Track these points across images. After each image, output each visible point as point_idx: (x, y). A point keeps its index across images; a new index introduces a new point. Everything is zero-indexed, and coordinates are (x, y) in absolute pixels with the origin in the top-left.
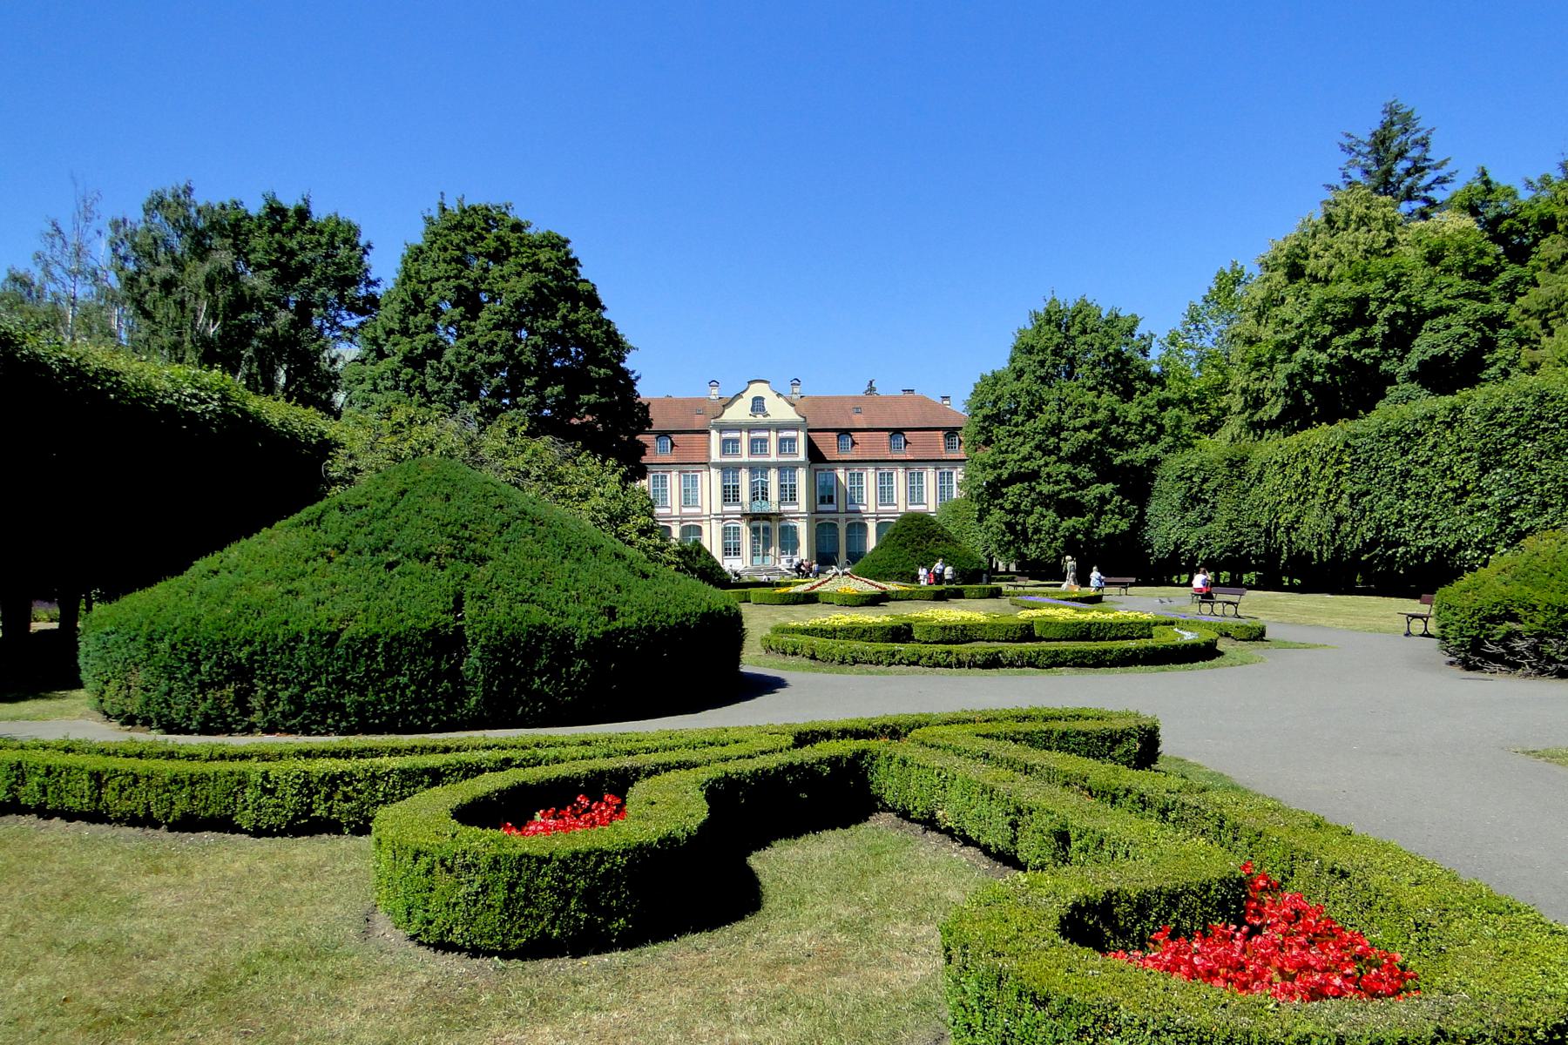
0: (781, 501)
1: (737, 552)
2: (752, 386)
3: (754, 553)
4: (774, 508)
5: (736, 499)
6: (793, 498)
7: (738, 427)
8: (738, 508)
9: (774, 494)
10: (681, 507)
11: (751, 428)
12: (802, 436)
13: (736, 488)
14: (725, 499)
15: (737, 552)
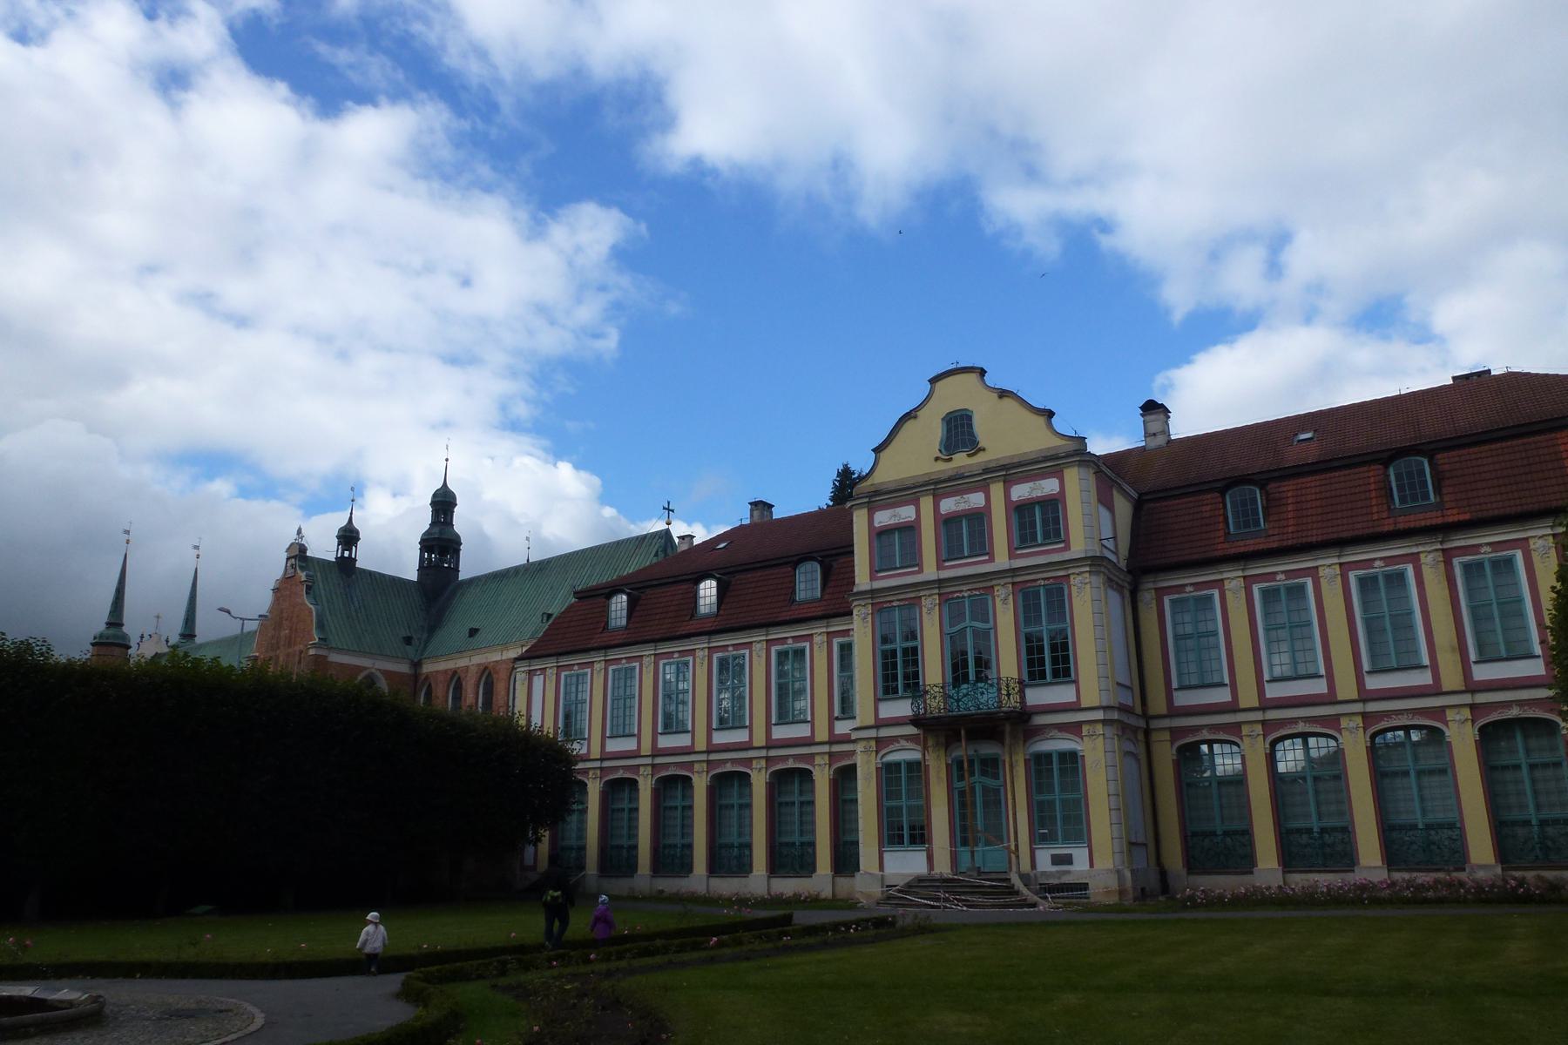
0: (1035, 672)
1: (920, 836)
2: (939, 385)
3: (963, 835)
4: (1013, 702)
5: (914, 686)
6: (1063, 670)
7: (907, 492)
8: (902, 708)
9: (1008, 662)
10: (832, 720)
11: (938, 487)
12: (1076, 487)
13: (913, 656)
14: (888, 689)
15: (920, 836)
